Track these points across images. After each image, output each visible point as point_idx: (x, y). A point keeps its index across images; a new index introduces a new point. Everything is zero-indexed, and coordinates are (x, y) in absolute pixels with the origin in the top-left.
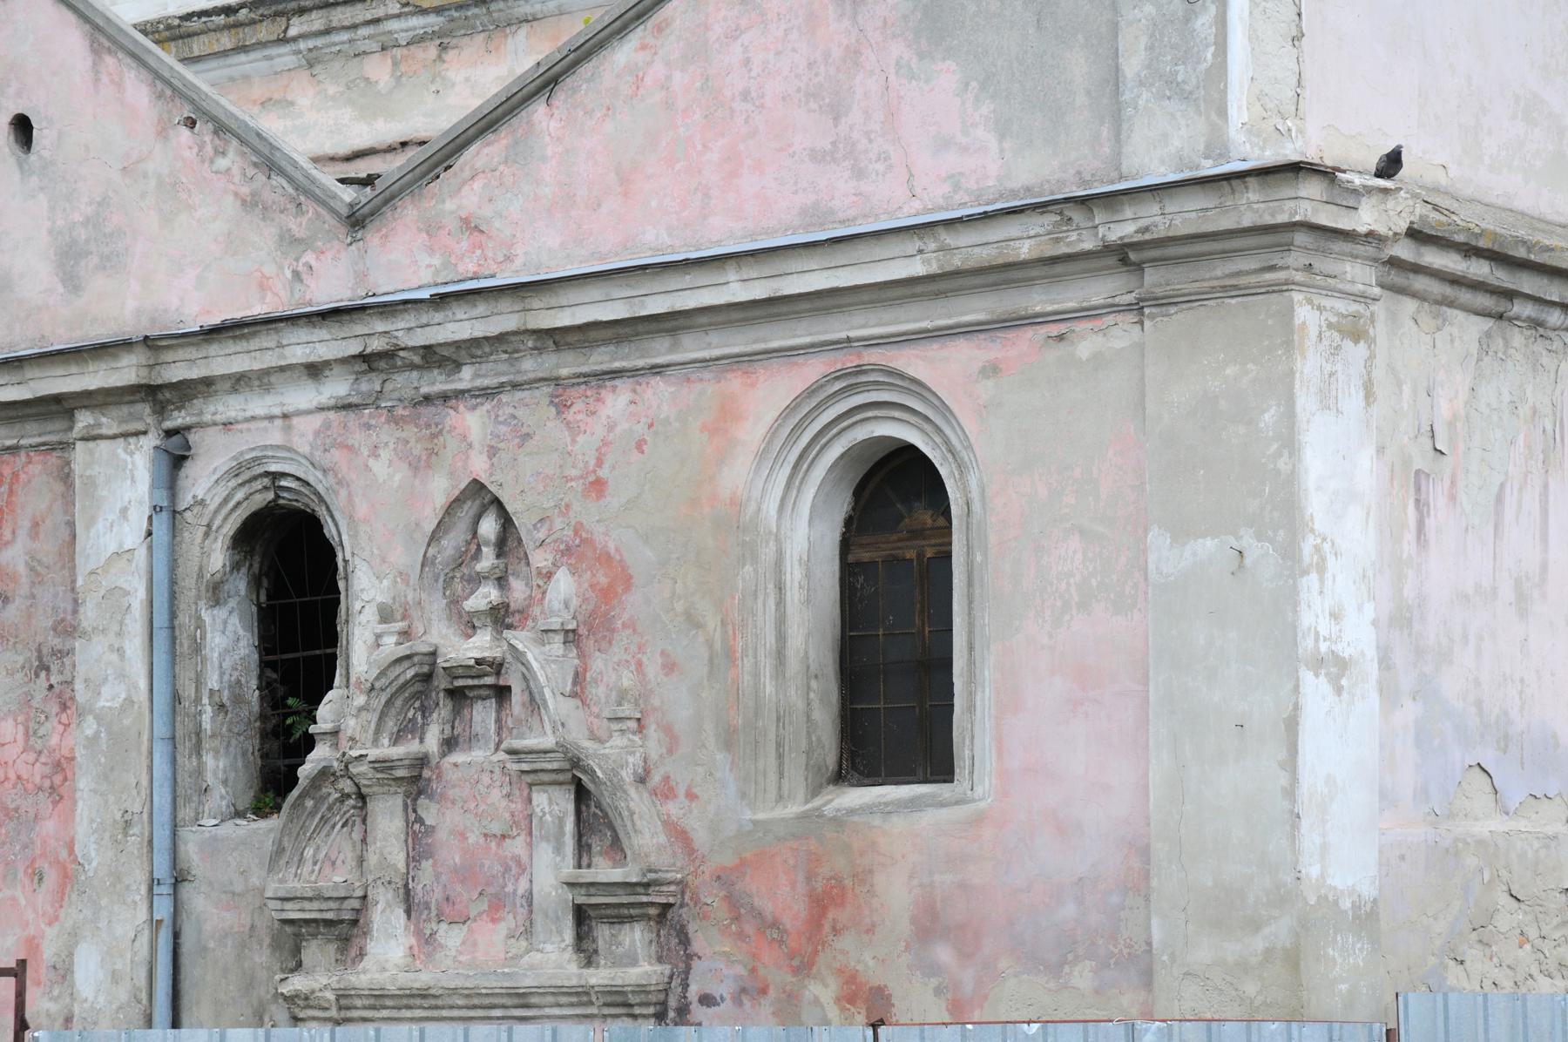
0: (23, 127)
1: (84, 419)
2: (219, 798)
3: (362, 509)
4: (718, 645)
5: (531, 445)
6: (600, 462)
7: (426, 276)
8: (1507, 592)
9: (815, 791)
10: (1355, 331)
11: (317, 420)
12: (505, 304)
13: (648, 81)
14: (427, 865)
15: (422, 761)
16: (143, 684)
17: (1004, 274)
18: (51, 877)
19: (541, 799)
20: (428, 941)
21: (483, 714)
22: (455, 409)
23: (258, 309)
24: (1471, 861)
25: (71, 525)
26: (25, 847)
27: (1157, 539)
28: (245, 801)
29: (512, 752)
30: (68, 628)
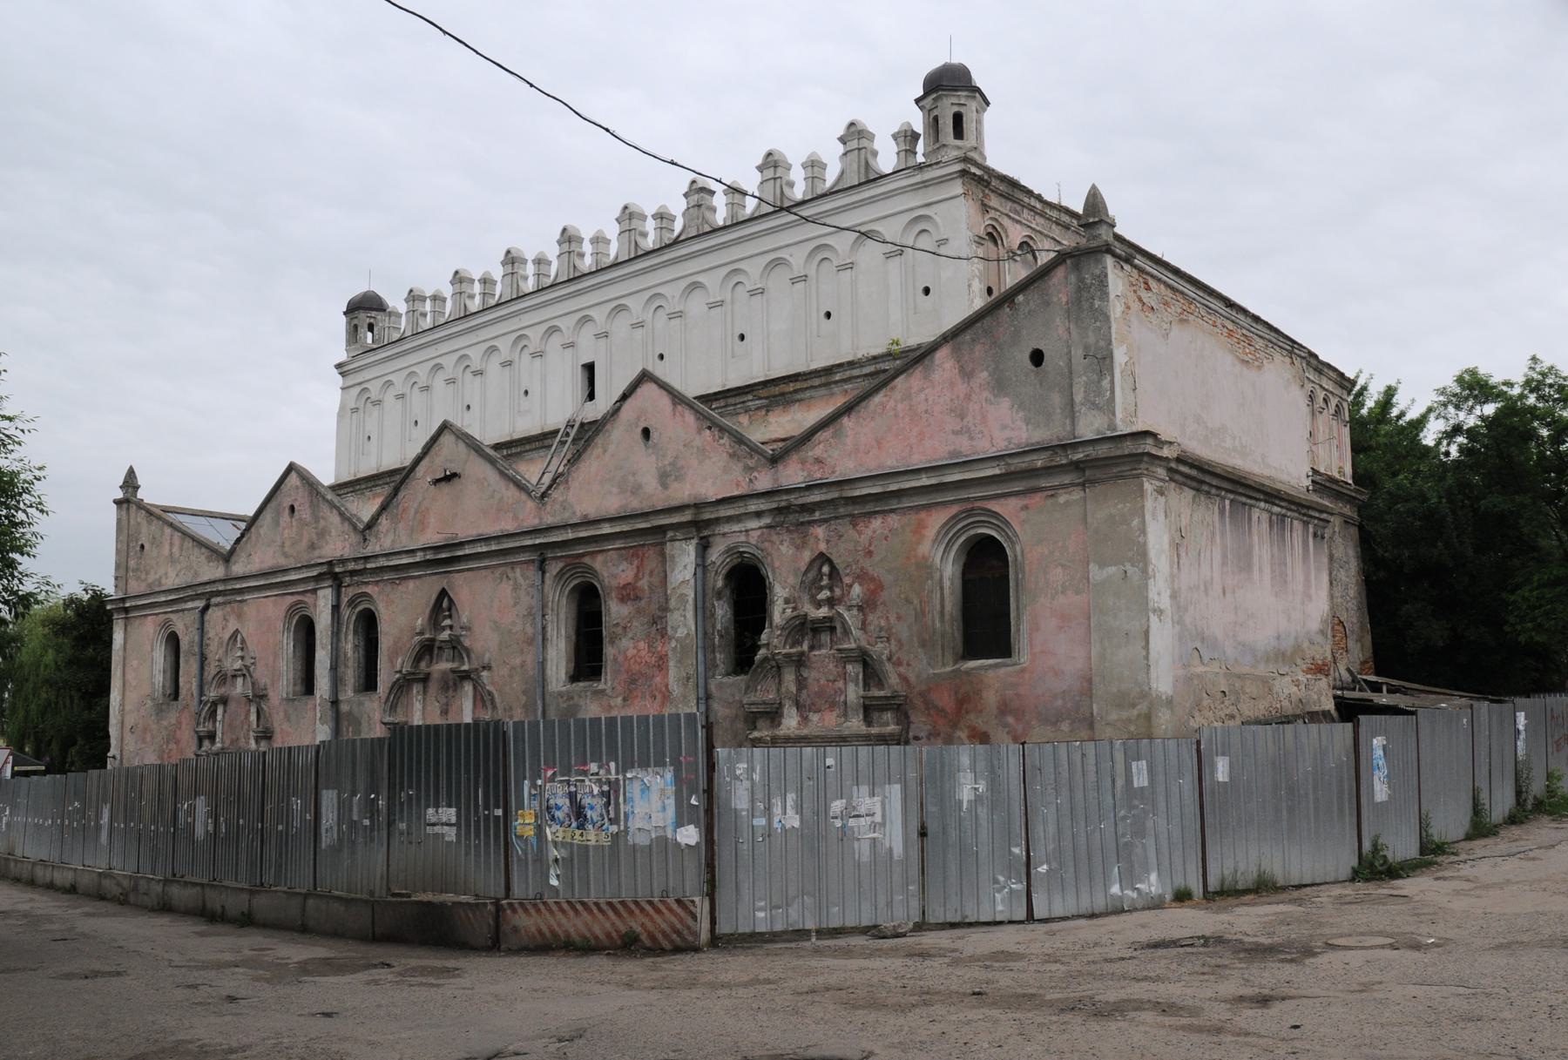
0: (646, 433)
1: (670, 534)
2: (722, 668)
3: (777, 564)
4: (919, 609)
5: (843, 539)
6: (870, 545)
7: (801, 479)
8: (1202, 588)
9: (955, 662)
10: (1161, 492)
11: (759, 532)
12: (833, 489)
14: (805, 692)
15: (802, 654)
16: (693, 628)
17: (1032, 473)
18: (659, 697)
19: (849, 667)
20: (805, 720)
21: (825, 638)
23: (736, 493)
24: (1196, 682)
25: (665, 572)
26: (649, 687)
27: (1093, 567)
28: (730, 670)
29: (838, 650)
30: (665, 609)
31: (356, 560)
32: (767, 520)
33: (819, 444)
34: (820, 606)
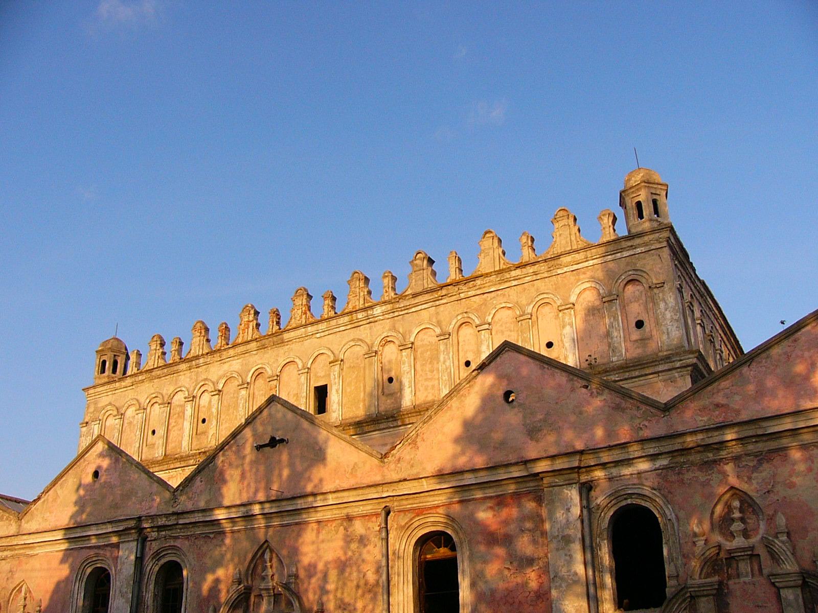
13: (794, 355)
22: (719, 465)
31: (167, 516)
33: (718, 392)
34: (734, 537)
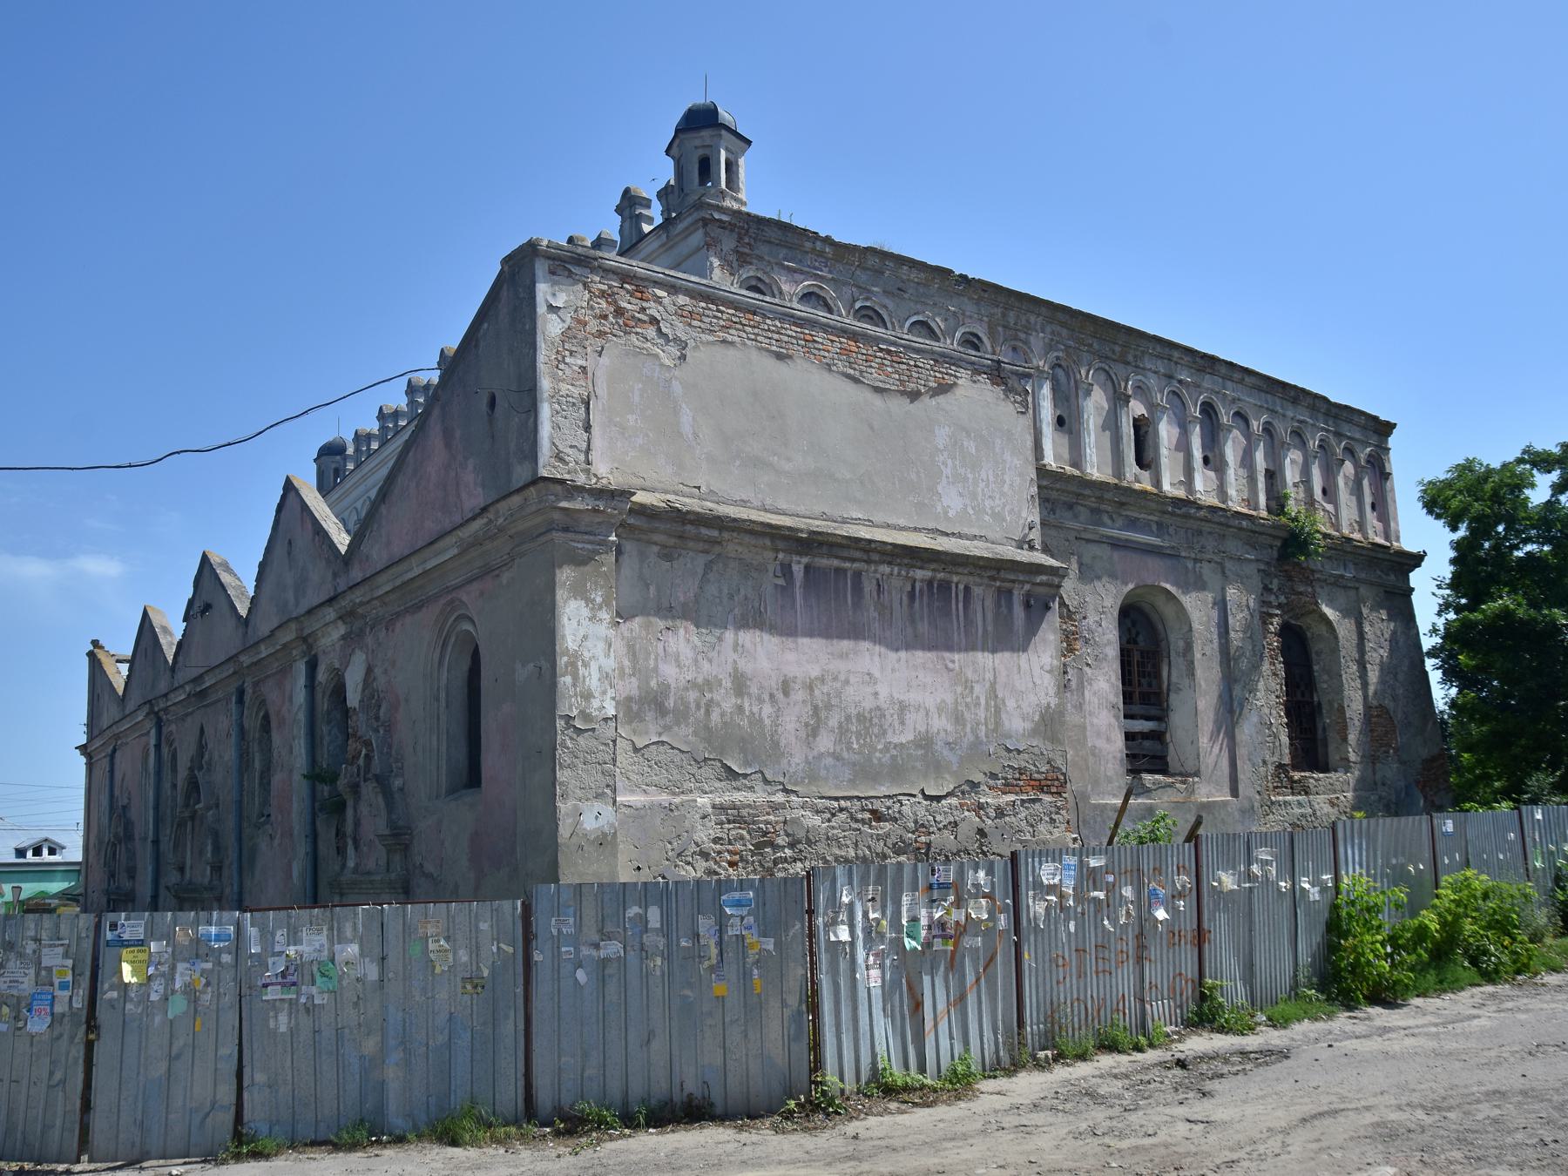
8: (727, 683)
32: (342, 629)
